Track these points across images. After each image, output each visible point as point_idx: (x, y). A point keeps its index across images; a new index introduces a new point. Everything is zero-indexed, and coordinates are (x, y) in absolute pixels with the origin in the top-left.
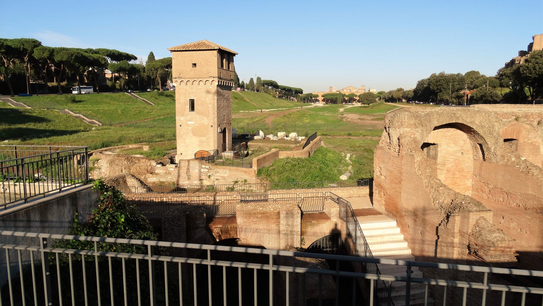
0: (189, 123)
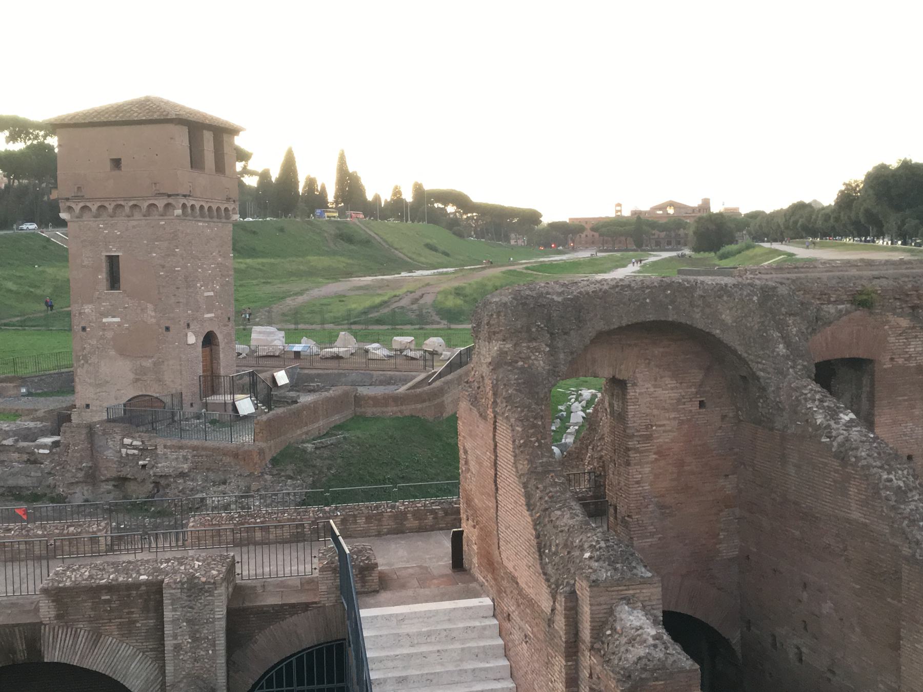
0: (104, 320)
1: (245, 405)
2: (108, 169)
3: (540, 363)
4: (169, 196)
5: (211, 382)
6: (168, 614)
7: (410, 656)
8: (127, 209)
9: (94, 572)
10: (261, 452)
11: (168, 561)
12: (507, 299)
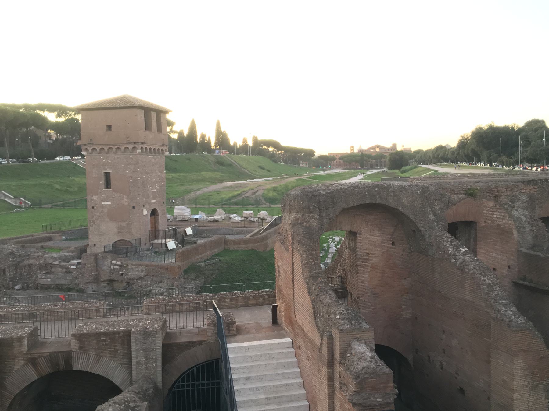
0: (103, 203)
1: (171, 244)
2: (105, 130)
3: (315, 224)
4: (135, 143)
5: (155, 233)
6: (133, 347)
7: (252, 367)
8: (114, 150)
9: (97, 326)
10: (179, 267)
11: (133, 321)
12: (297, 193)
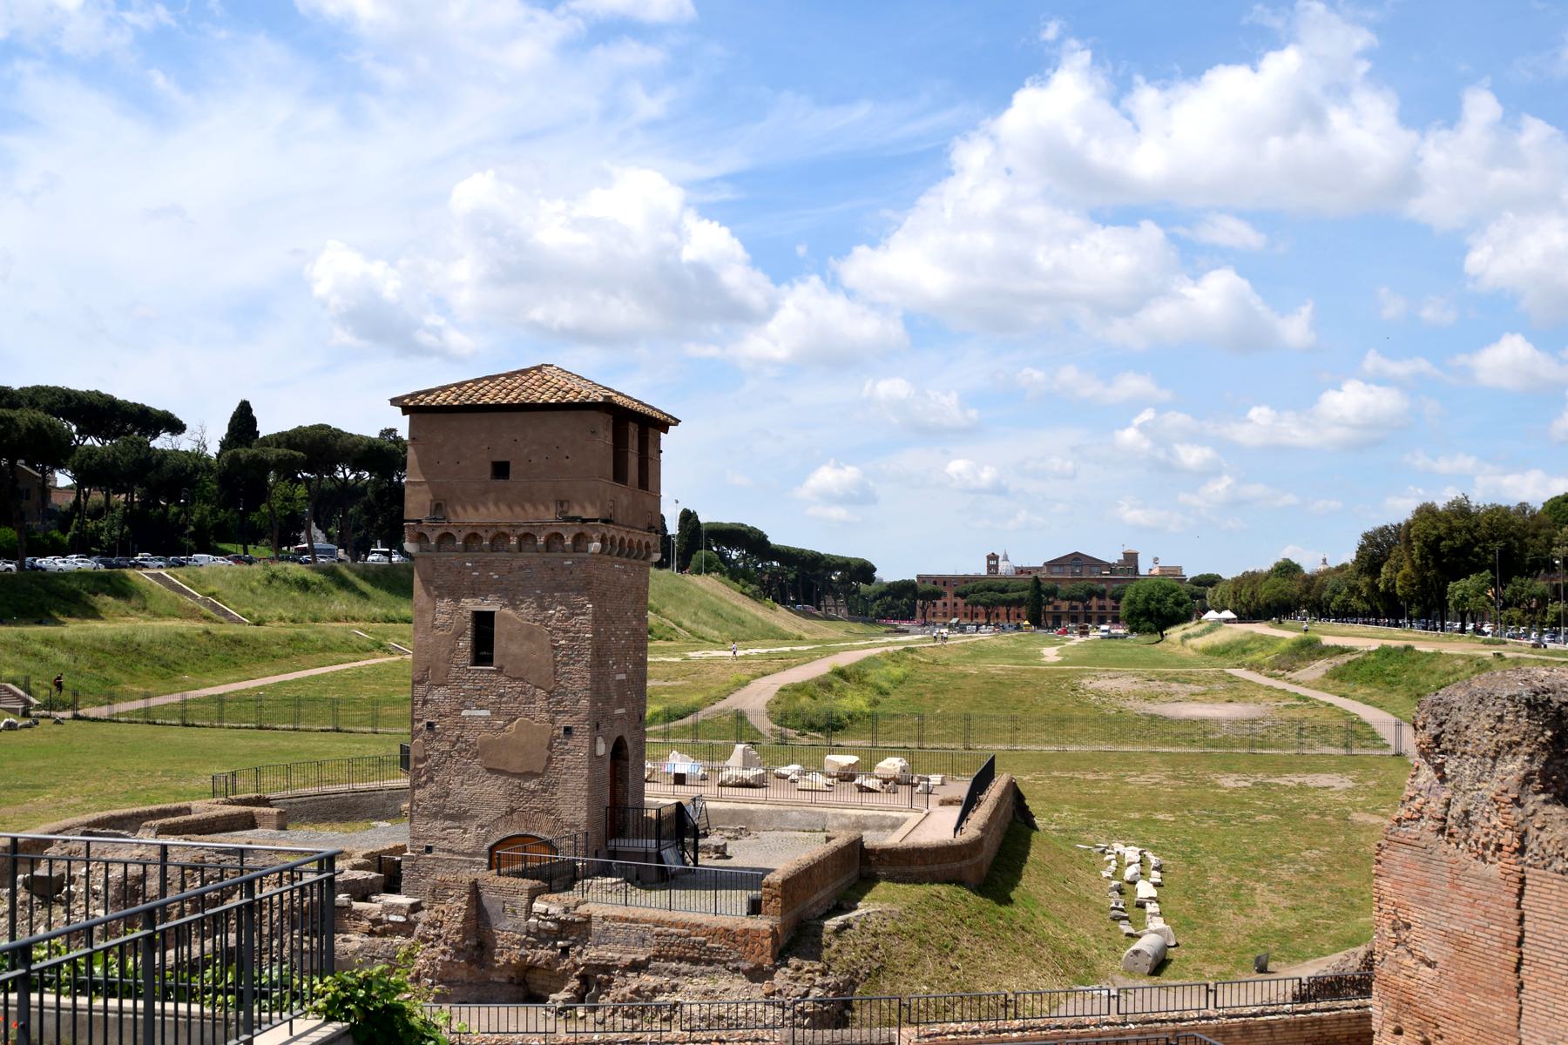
2: (488, 475)
